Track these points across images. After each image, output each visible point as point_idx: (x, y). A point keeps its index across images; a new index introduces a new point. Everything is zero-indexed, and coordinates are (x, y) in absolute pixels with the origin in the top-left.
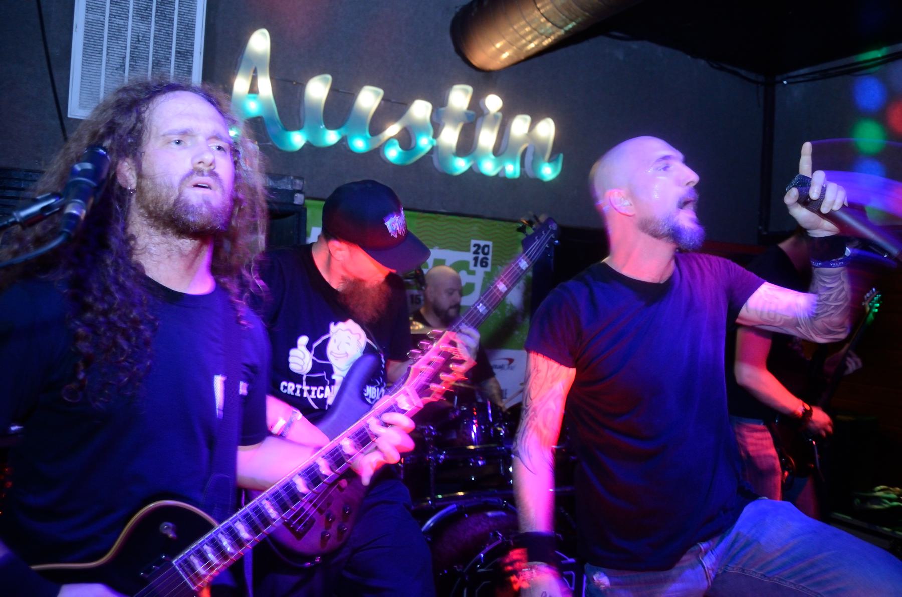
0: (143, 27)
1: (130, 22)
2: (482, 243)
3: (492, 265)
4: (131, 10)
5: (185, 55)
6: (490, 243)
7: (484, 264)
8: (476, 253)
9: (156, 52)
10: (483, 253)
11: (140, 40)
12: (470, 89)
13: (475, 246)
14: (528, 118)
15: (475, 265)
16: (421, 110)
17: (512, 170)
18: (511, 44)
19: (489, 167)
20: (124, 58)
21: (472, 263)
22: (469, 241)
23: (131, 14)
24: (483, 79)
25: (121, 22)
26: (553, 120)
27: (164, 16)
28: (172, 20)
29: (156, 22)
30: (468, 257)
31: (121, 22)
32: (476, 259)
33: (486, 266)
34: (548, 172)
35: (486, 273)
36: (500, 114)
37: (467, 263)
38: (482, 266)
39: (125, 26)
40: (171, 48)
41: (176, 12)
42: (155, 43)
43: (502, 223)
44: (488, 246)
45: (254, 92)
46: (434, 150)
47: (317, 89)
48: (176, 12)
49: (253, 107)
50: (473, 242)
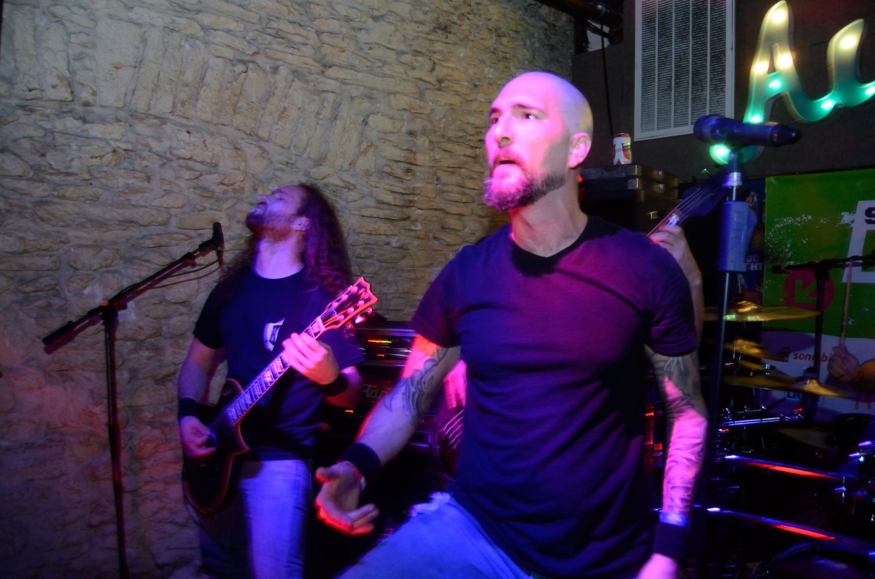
0: (683, 46)
1: (673, 46)
4: (674, 36)
5: (719, 57)
9: (694, 63)
11: (682, 57)
20: (671, 79)
25: (666, 49)
27: (699, 29)
31: (666, 49)
39: (670, 51)
40: (706, 55)
42: (694, 56)
45: (774, 70)
47: (846, 41)
49: (776, 86)
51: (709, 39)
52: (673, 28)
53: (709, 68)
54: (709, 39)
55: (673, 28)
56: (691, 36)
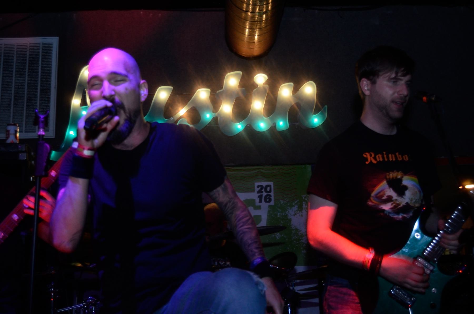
1: (14, 79)
2: (264, 184)
3: (275, 200)
4: (14, 72)
5: (46, 91)
6: (271, 183)
7: (268, 199)
8: (260, 192)
10: (266, 191)
12: (240, 73)
13: (258, 187)
14: (292, 84)
15: (260, 201)
16: (203, 94)
17: (282, 124)
18: (252, 35)
19: (262, 126)
21: (257, 200)
22: (254, 184)
23: (14, 74)
24: (246, 65)
26: (315, 82)
28: (37, 73)
29: (28, 75)
30: (254, 196)
32: (260, 197)
33: (270, 200)
34: (316, 120)
35: (269, 206)
36: (267, 86)
37: (253, 200)
38: (266, 201)
40: (37, 89)
41: (40, 67)
42: (28, 88)
43: (281, 167)
44: (270, 186)
46: (215, 120)
48: (40, 67)
50: (257, 184)
51: (39, 79)
52: (14, 67)
53: (39, 97)
54: (39, 79)
55: (14, 67)
56: (27, 74)
